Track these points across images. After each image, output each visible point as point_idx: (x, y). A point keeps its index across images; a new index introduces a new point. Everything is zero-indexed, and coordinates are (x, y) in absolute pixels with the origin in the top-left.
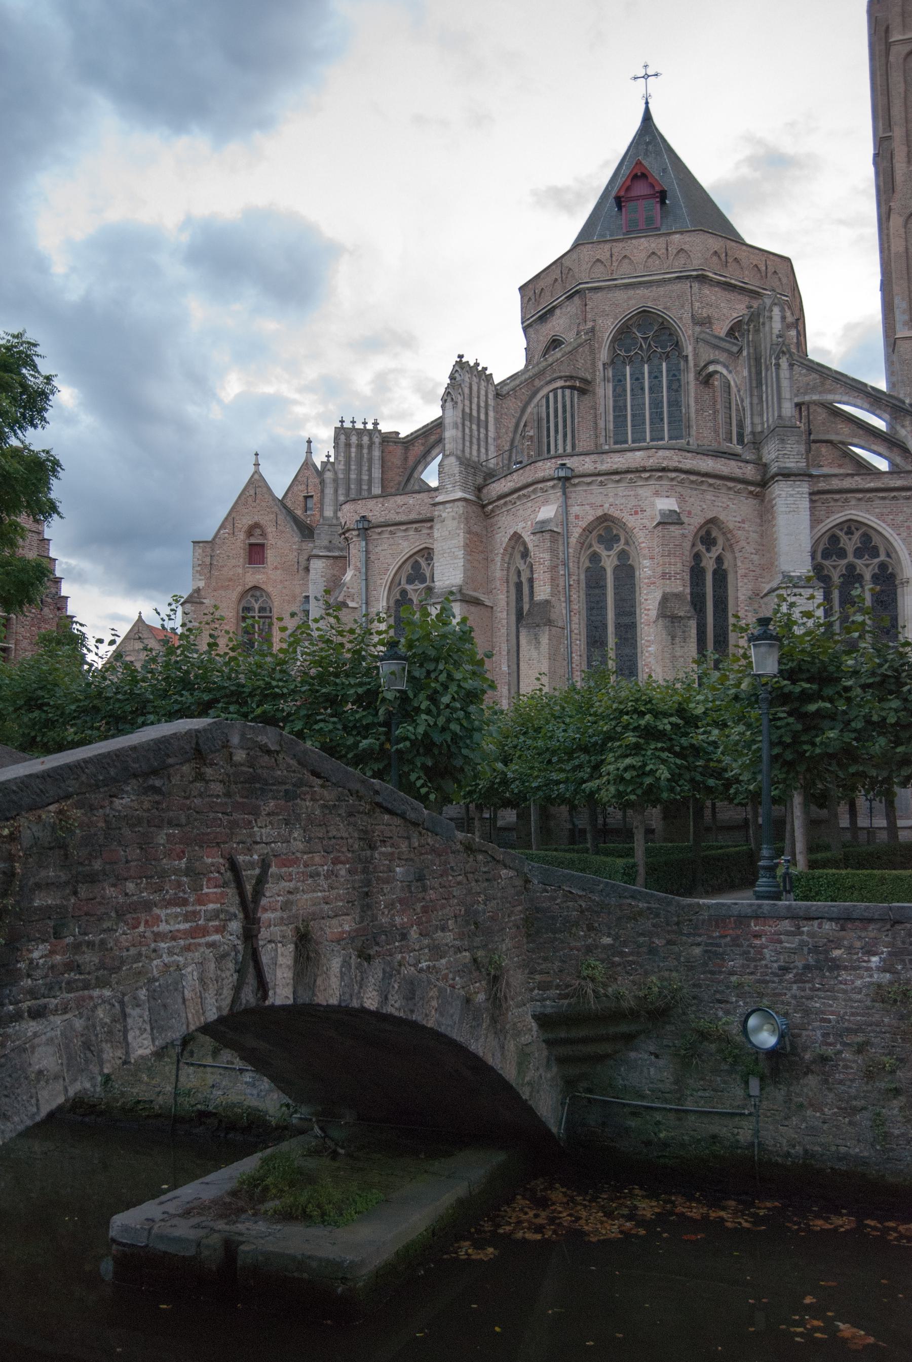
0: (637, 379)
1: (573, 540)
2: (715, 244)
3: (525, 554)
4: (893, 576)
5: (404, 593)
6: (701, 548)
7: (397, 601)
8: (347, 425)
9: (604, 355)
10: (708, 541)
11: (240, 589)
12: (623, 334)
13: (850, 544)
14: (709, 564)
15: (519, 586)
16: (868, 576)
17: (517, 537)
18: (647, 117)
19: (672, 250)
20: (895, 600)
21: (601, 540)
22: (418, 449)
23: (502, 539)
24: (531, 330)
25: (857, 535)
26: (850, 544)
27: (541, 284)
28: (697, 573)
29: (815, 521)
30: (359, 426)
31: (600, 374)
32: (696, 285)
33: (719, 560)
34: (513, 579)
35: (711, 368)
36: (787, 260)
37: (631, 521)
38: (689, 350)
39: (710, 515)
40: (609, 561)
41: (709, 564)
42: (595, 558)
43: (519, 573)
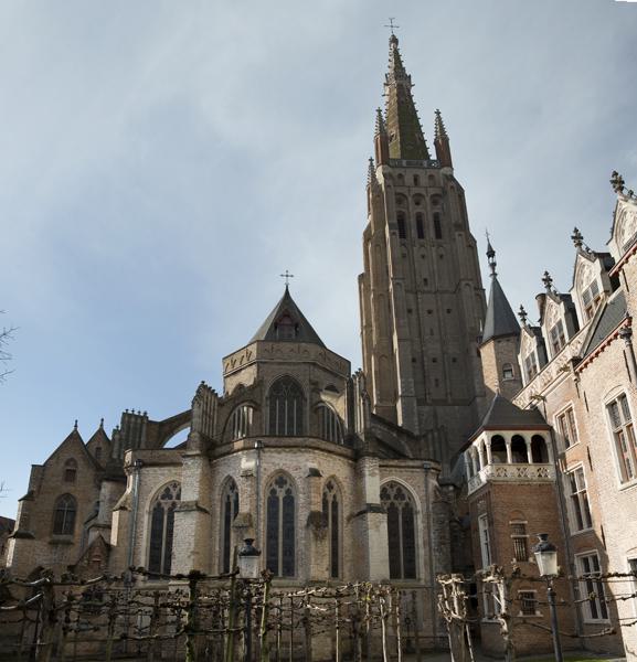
0: (282, 404)
1: (262, 482)
2: (320, 349)
3: (234, 487)
4: (412, 509)
5: (159, 504)
6: (327, 490)
7: (155, 509)
8: (130, 412)
9: (267, 393)
10: (330, 486)
11: (58, 494)
12: (276, 386)
13: (392, 493)
14: (330, 499)
15: (228, 504)
16: (400, 508)
17: (230, 478)
18: (287, 293)
19: (302, 350)
20: (412, 521)
21: (277, 483)
22: (167, 428)
23: (220, 478)
24: (228, 379)
25: (395, 489)
26: (392, 493)
27: (235, 357)
28: (325, 502)
29: (381, 479)
30: (136, 413)
31: (264, 404)
32: (312, 367)
33: (335, 497)
34: (225, 500)
35: (320, 405)
36: (349, 363)
37: (294, 474)
38: (307, 395)
39: (332, 473)
40: (281, 494)
41: (330, 499)
42: (273, 492)
43: (228, 497)
